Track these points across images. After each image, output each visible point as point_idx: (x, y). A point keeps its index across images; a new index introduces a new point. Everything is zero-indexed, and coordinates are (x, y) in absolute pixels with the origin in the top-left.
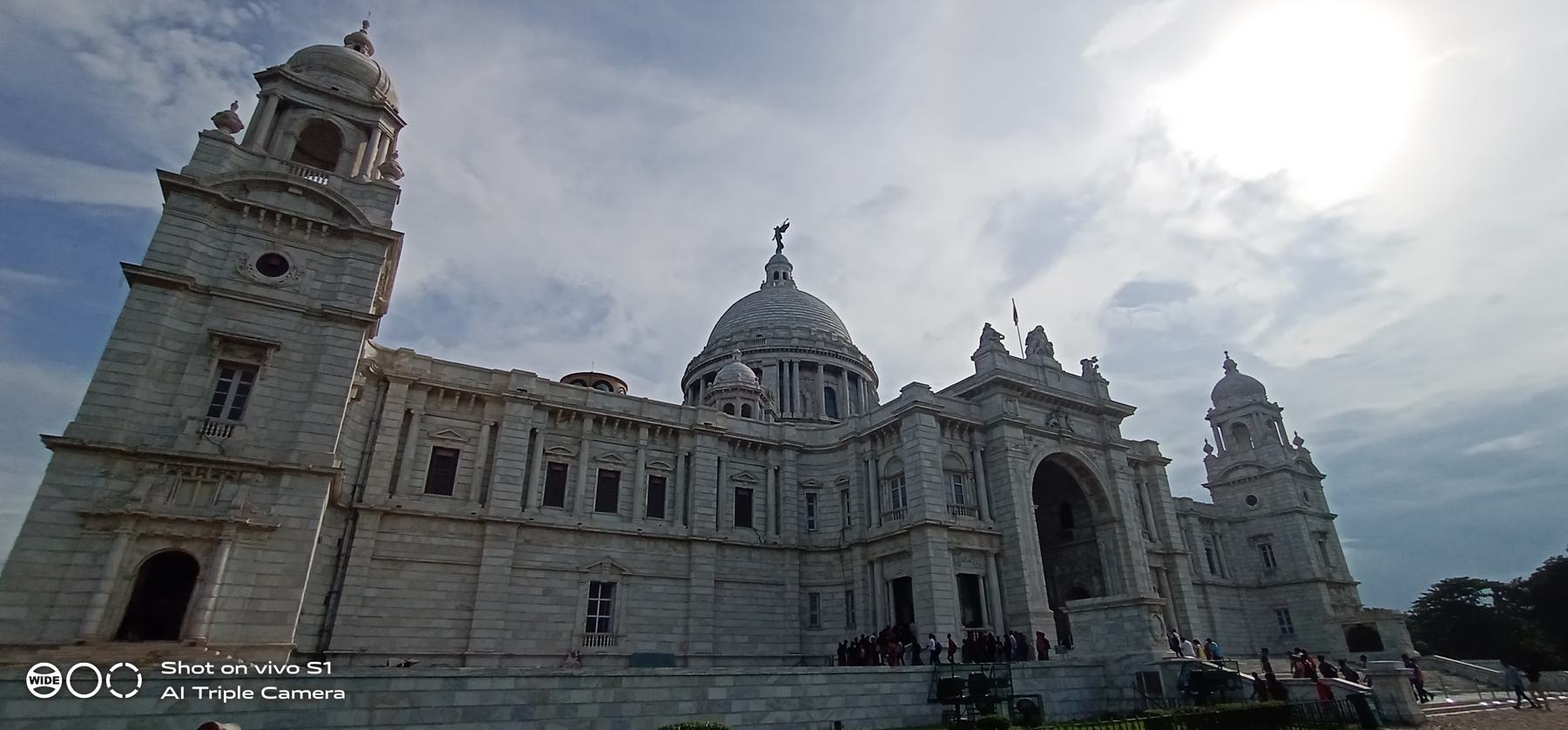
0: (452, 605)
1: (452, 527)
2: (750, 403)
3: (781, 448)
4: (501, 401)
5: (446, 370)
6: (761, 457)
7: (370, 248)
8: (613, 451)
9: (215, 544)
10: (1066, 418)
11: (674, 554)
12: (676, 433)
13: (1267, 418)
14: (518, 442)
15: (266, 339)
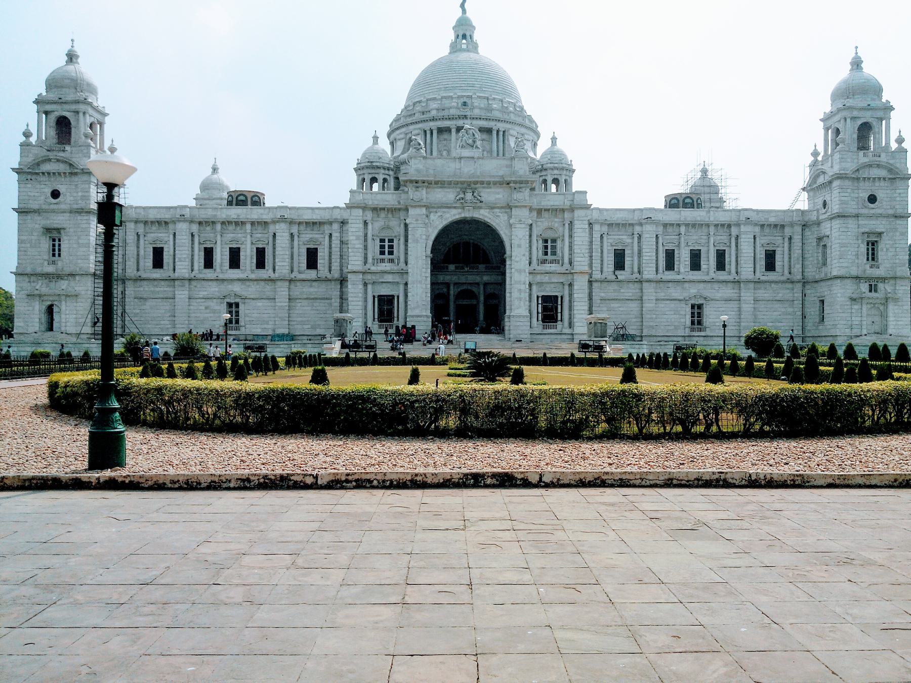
0: (169, 314)
1: (163, 283)
2: (376, 176)
3: (331, 223)
4: (174, 222)
5: (151, 211)
6: (322, 228)
7: (85, 178)
8: (234, 237)
9: (60, 301)
10: (473, 192)
11: (268, 287)
12: (266, 224)
13: (859, 122)
14: (184, 241)
15: (59, 226)
